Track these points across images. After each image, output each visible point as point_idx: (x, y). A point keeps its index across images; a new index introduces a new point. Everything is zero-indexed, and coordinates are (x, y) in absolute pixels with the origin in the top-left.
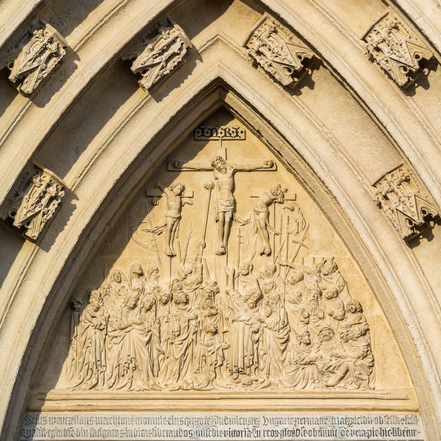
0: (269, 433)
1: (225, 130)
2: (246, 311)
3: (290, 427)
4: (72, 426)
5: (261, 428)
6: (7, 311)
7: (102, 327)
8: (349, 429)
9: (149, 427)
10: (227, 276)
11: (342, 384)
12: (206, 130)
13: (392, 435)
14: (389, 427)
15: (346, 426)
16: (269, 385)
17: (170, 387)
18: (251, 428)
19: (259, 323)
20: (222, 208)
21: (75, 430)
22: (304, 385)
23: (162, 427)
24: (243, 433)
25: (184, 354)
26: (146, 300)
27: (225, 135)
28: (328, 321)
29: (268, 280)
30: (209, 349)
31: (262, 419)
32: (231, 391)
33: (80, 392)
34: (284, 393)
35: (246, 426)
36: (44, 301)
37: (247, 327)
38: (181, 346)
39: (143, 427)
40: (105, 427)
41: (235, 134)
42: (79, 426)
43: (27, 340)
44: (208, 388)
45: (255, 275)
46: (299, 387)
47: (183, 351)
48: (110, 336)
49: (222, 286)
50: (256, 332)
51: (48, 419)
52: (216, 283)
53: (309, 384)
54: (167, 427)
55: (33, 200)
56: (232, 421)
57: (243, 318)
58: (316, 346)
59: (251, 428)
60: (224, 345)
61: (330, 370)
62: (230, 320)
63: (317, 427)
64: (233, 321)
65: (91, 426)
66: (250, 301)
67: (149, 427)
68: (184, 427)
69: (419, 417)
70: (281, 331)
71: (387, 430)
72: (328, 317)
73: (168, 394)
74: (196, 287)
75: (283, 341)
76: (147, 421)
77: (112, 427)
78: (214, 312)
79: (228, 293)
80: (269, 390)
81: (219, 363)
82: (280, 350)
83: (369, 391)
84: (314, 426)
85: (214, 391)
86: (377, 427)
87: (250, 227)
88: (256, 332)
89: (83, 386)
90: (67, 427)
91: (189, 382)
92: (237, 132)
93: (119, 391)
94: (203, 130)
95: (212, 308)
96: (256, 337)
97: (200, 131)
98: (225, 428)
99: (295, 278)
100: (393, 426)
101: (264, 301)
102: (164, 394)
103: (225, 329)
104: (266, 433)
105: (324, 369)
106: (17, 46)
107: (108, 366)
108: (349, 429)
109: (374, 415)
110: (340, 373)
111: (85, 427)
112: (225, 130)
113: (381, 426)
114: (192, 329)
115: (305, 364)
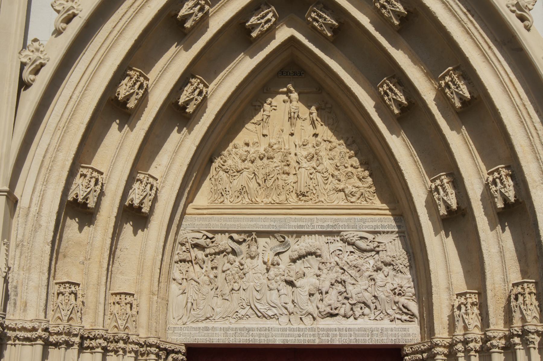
0: (320, 227)
1: (294, 72)
2: (306, 163)
3: (331, 224)
4: (210, 222)
5: (315, 224)
6: (174, 155)
7: (227, 171)
8: (364, 225)
9: (252, 223)
10: (296, 146)
11: (359, 201)
12: (284, 72)
13: (387, 228)
14: (386, 224)
15: (362, 223)
16: (319, 201)
17: (265, 202)
18: (309, 224)
19: (313, 169)
20: (293, 110)
21: (212, 225)
22: (338, 202)
23: (260, 223)
24: (305, 227)
25: (272, 185)
26: (251, 156)
27: (294, 75)
28: (350, 169)
29: (317, 148)
30: (286, 182)
31: (315, 220)
32: (298, 204)
33: (215, 204)
34: (327, 206)
35: (306, 223)
36: (195, 148)
37: (307, 171)
38: (270, 181)
39: (249, 223)
40: (228, 223)
41: (299, 74)
42: (214, 223)
43: (185, 169)
44: (286, 202)
45: (310, 145)
46: (335, 203)
47: (271, 183)
48: (231, 176)
49: (293, 151)
50: (311, 174)
51: (197, 218)
52: (289, 149)
53: (340, 202)
54: (263, 223)
55: (190, 91)
56: (300, 220)
57: (304, 166)
58: (344, 182)
59: (309, 224)
60: (294, 181)
61: (352, 194)
62: (297, 169)
63: (346, 224)
64: (299, 168)
65: (220, 223)
66: (308, 158)
67: (252, 223)
68: (272, 223)
69: (402, 218)
70: (325, 174)
71: (385, 225)
72: (350, 167)
73: (263, 206)
74: (278, 151)
75: (326, 178)
76: (252, 220)
77: (232, 223)
78: (288, 163)
79: (296, 155)
80: (319, 204)
81: (291, 190)
82: (324, 183)
83: (374, 205)
84: (344, 223)
85: (289, 204)
86: (379, 224)
87: (308, 122)
88: (311, 174)
89: (216, 202)
90: (207, 223)
91: (275, 199)
92: (300, 73)
93: (236, 204)
94: (282, 72)
95: (288, 161)
96: (312, 176)
97: (281, 72)
98: (295, 224)
99: (332, 146)
100: (388, 223)
101: (315, 158)
102: (261, 206)
103: (294, 172)
104: (318, 227)
105: (349, 193)
106: (182, 2)
107: (230, 192)
108: (364, 225)
109: (378, 217)
110: (358, 195)
111: (217, 223)
112: (294, 72)
113: (381, 223)
114: (276, 172)
115: (338, 191)
